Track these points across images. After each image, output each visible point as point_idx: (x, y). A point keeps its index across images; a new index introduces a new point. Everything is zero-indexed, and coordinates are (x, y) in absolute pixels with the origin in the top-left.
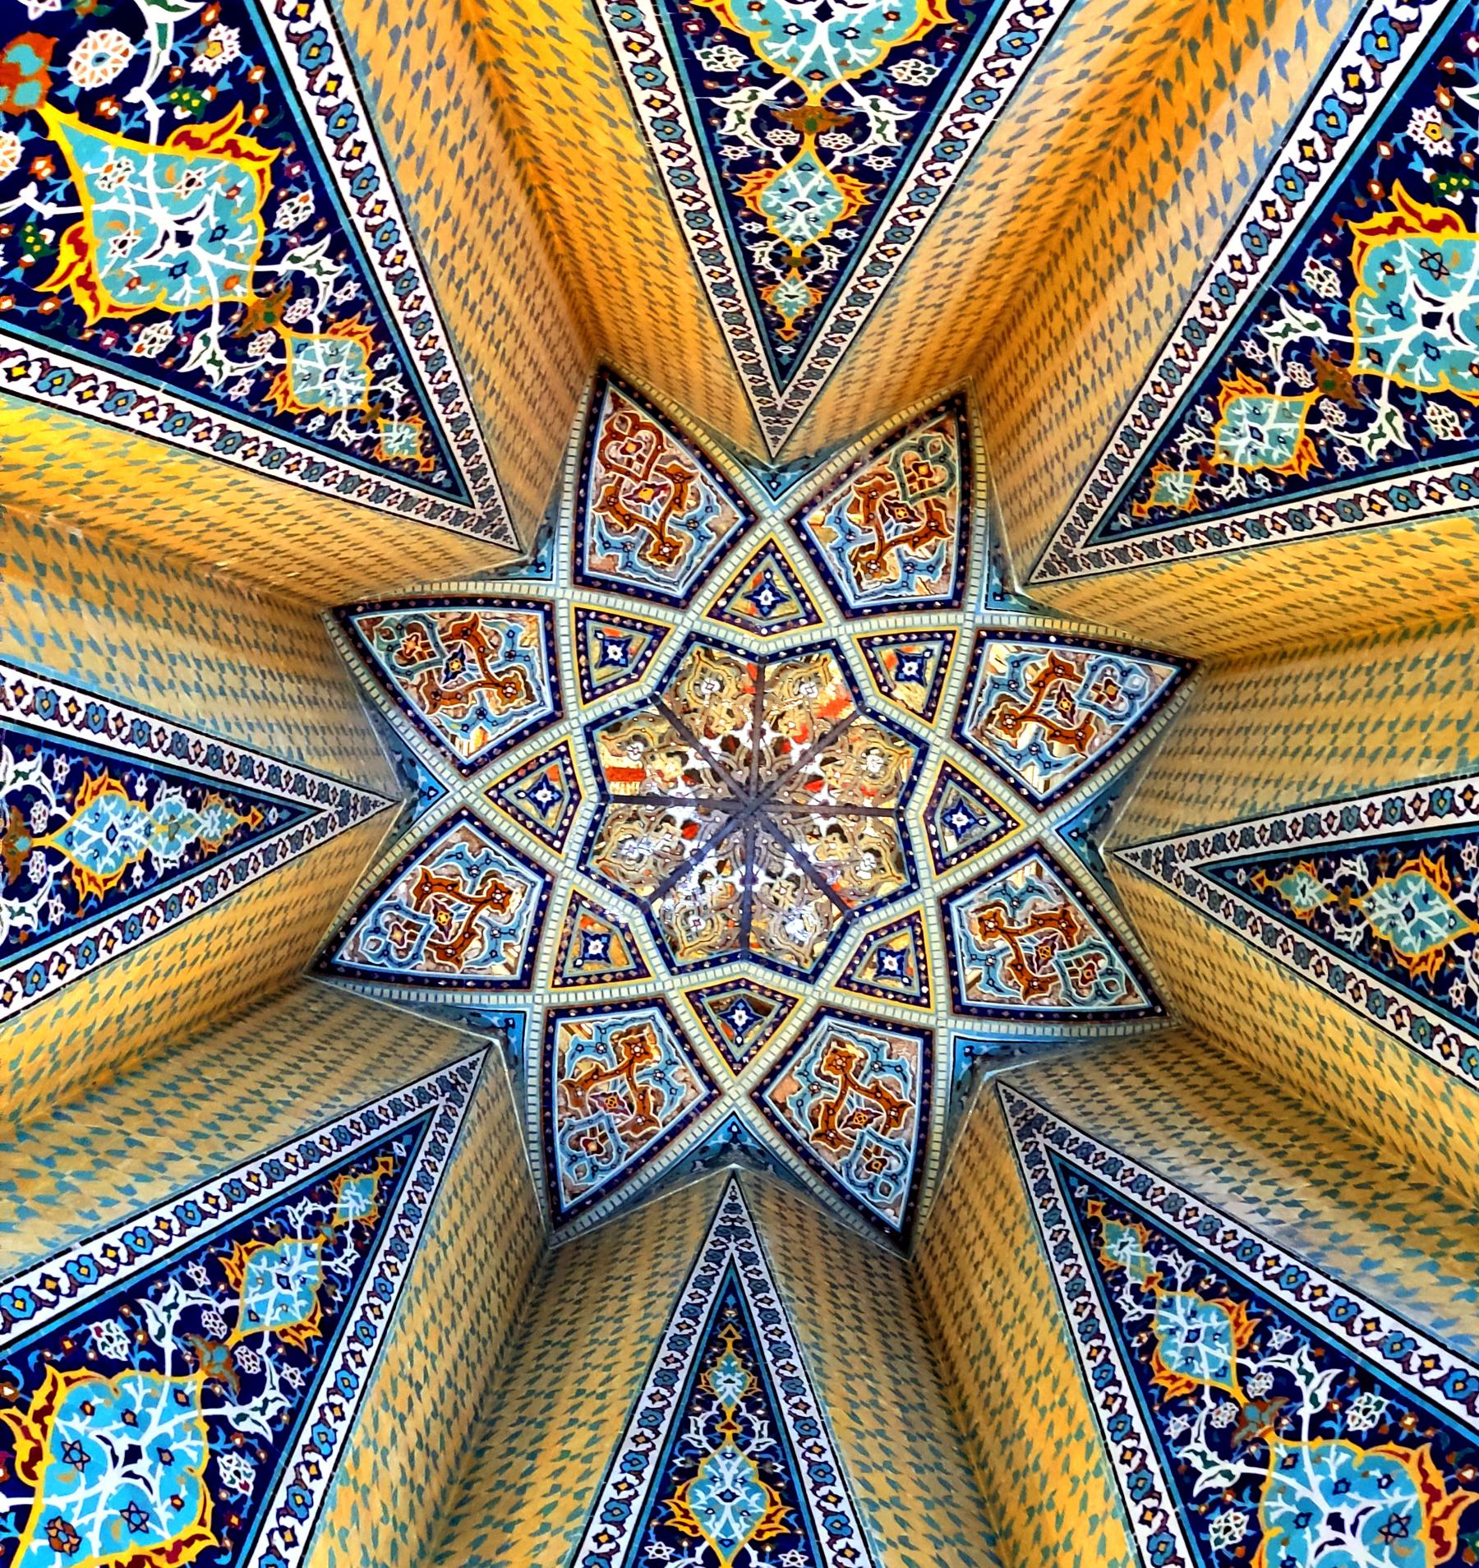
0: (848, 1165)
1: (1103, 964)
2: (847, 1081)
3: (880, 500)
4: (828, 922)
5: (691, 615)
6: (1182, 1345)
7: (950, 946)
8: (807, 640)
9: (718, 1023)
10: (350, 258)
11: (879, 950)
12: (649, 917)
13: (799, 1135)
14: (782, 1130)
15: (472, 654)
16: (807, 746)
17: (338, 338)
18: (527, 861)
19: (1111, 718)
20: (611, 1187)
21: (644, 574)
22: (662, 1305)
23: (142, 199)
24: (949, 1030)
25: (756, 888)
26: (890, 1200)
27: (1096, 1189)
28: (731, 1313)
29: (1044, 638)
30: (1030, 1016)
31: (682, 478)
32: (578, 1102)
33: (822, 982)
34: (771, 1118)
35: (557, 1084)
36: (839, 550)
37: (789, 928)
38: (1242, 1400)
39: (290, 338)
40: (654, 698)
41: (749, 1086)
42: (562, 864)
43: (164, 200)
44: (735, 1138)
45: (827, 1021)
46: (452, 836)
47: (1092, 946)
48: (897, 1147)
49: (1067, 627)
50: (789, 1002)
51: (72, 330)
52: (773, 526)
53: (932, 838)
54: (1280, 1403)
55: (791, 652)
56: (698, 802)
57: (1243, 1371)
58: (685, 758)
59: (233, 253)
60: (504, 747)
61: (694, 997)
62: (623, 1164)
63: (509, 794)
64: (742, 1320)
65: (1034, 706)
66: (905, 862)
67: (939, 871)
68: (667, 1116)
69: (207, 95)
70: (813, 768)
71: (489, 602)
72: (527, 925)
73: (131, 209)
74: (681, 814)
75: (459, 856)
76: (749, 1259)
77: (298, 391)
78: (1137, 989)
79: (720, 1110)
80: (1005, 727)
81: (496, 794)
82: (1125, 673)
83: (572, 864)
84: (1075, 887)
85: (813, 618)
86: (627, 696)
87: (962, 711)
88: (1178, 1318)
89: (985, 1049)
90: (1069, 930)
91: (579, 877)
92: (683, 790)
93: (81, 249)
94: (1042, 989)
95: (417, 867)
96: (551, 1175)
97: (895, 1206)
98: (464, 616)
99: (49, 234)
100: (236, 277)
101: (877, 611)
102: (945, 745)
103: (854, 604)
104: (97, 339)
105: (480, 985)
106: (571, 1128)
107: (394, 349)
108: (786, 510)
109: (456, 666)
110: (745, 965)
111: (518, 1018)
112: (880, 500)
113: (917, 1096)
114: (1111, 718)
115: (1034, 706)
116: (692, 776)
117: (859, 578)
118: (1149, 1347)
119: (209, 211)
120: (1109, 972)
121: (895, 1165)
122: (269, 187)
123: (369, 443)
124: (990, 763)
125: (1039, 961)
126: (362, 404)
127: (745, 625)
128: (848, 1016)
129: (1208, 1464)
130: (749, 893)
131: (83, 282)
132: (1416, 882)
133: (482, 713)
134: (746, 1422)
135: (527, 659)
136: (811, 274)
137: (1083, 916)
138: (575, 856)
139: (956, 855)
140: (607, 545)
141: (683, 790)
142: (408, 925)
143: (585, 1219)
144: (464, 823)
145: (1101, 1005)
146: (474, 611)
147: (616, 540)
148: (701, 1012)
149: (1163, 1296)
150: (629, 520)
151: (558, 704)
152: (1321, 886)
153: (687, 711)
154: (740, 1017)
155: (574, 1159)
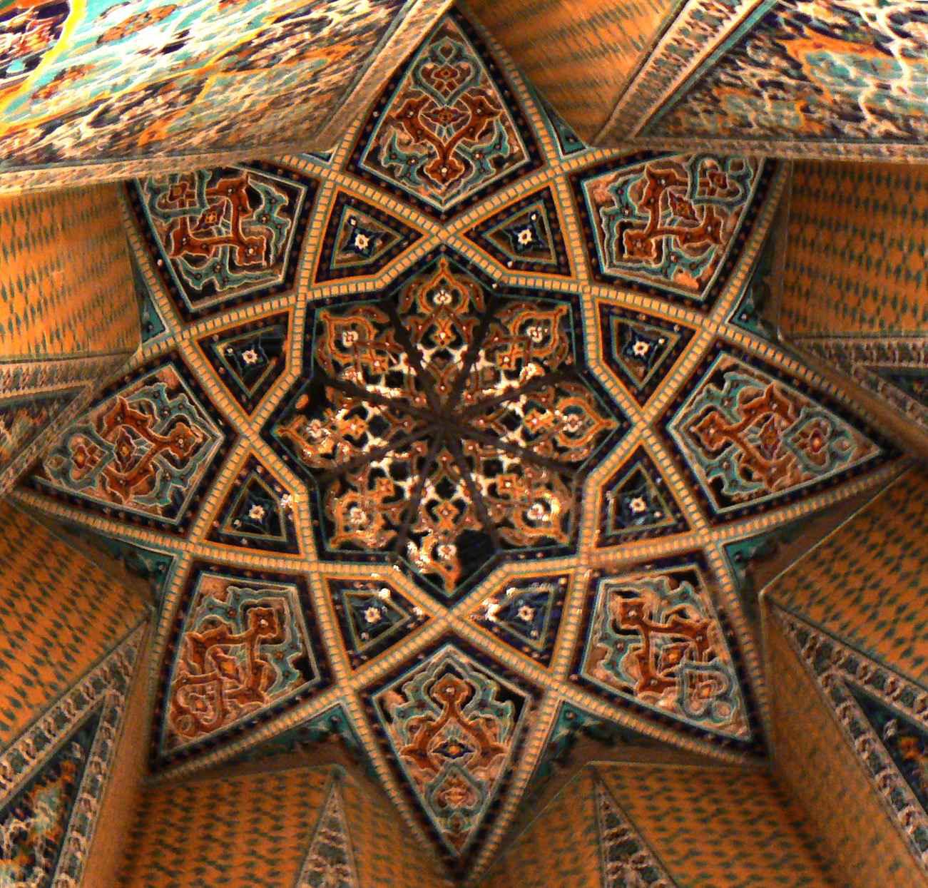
0: (730, 205)
2: (654, 231)
3: (123, 474)
5: (306, 567)
7: (483, 195)
8: (272, 458)
11: (517, 252)
14: (726, 273)
15: (437, 741)
18: (589, 602)
20: (846, 414)
21: (295, 630)
25: (515, 384)
30: (512, 101)
31: (200, 647)
32: (782, 470)
33: (573, 288)
34: (720, 286)
35: (774, 494)
36: (183, 479)
41: (698, 318)
44: (752, 316)
46: (599, 675)
47: (418, 83)
48: (693, 168)
49: (142, 259)
53: (390, 256)
58: (432, 504)
61: (642, 397)
62: (819, 408)
66: (425, 267)
67: (419, 235)
68: (757, 386)
70: (382, 388)
71: (386, 748)
75: (612, 665)
79: (733, 334)
80: (258, 252)
85: (252, 463)
87: (264, 295)
91: (583, 548)
94: (481, 104)
95: (638, 699)
96: (857, 472)
101: (217, 415)
102: (302, 290)
103: (221, 437)
106: (807, 468)
108: (176, 544)
110: (592, 364)
111: (733, 550)
112: (123, 474)
113: (637, 166)
115: (227, 241)
116: (445, 490)
117: (198, 447)
120: (434, 58)
124: (297, 247)
125: (454, 116)
128: (592, 253)
137: (395, 100)
142: (693, 686)
144: (584, 673)
145: (470, 51)
146: (401, 757)
147: (278, 670)
150: (257, 669)
155: (835, 456)
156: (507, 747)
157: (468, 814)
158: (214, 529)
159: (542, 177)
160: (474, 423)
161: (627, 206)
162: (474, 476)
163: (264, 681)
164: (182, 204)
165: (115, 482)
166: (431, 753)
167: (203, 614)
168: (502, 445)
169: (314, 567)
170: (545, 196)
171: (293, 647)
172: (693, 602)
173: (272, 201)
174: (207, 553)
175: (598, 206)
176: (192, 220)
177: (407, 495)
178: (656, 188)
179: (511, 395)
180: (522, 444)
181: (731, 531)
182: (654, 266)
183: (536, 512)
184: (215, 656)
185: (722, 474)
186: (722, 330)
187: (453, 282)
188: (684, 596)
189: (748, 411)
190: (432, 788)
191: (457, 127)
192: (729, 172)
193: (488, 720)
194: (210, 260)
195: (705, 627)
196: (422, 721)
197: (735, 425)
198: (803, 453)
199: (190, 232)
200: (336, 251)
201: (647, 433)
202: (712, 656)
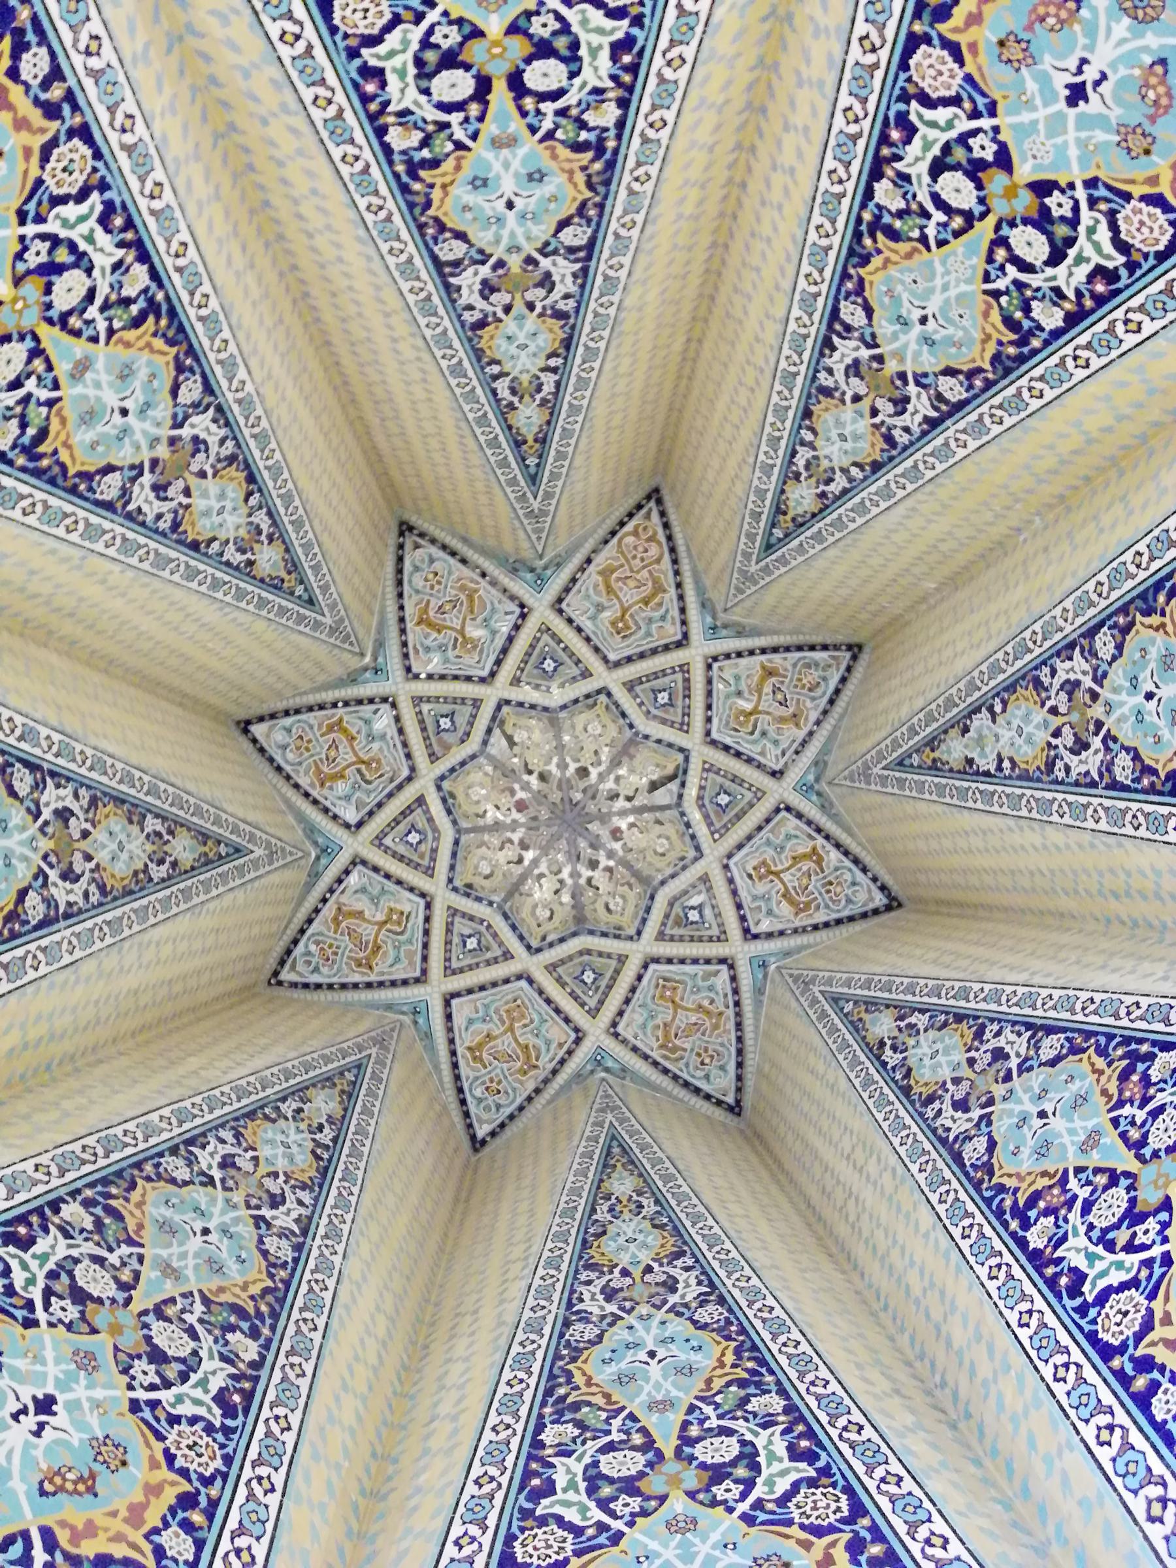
10: (924, 433)
17: (869, 437)
23: (945, 288)
38: (258, 1175)
39: (865, 405)
43: (947, 301)
51: (855, 260)
54: (265, 1196)
57: (276, 1175)
59: (917, 355)
69: (1018, 315)
73: (939, 282)
77: (829, 417)
93: (909, 256)
99: (916, 234)
100: (902, 360)
104: (850, 277)
107: (865, 478)
119: (943, 332)
122: (965, 368)
123: (797, 476)
126: (825, 464)
129: (212, 1155)
131: (887, 261)
149: (303, 1126)
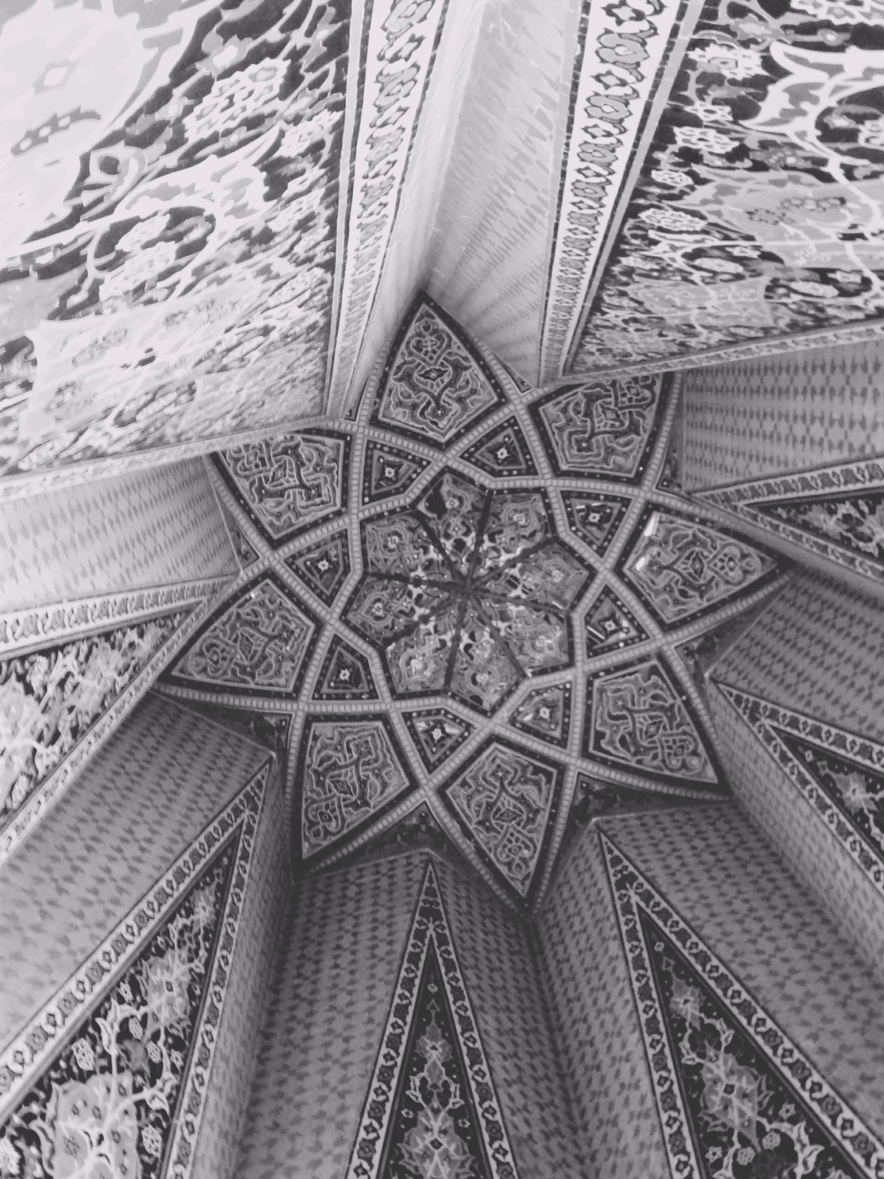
1: (526, 853)
2: (356, 763)
3: (697, 549)
4: (433, 680)
5: (555, 482)
6: (428, 1142)
7: (471, 760)
8: (586, 556)
9: (332, 667)
12: (361, 581)
13: (308, 761)
15: (446, 380)
16: (524, 596)
18: (345, 491)
19: (664, 761)
22: (197, 817)
24: (426, 795)
25: (422, 627)
26: (313, 840)
27: (442, 993)
28: (225, 861)
29: (682, 691)
31: (634, 428)
32: (233, 628)
33: (398, 704)
34: (304, 738)
35: (233, 609)
37: (380, 613)
40: (491, 491)
41: (312, 709)
42: (358, 511)
45: (379, 724)
46: (329, 441)
47: (531, 840)
48: (343, 820)
49: (697, 702)
50: (373, 695)
52: (640, 496)
55: (572, 551)
56: (447, 558)
58: (466, 534)
60: (403, 432)
61: (337, 640)
62: (219, 682)
63: (377, 454)
64: (228, 871)
65: (638, 712)
68: (261, 681)
71: (485, 368)
72: (309, 519)
74: (433, 554)
76: (250, 831)
78: (528, 883)
80: (615, 703)
81: (371, 446)
82: (695, 753)
83: (361, 516)
84: (556, 805)
85: (601, 551)
86: (482, 478)
87: (608, 671)
88: (436, 1124)
89: (432, 824)
90: (530, 821)
92: (449, 545)
94: (489, 829)
97: (313, 846)
98: (466, 359)
101: (631, 586)
102: (580, 675)
103: (625, 569)
105: (256, 522)
109: (433, 375)
110: (374, 654)
112: (697, 549)
114: (664, 761)
115: (638, 712)
116: (460, 545)
118: (412, 1123)
120: (524, 860)
121: (333, 826)
127: (570, 515)
130: (416, 624)
132: (748, 1083)
133: (414, 406)
134: (198, 943)
135: (465, 409)
136: (849, 535)
138: (367, 514)
139: (523, 724)
140: (565, 410)
141: (449, 545)
142: (262, 460)
143: (173, 690)
144: (342, 443)
145: (504, 870)
146: (473, 363)
147: (572, 413)
148: (331, 651)
150: (588, 414)
151: (450, 443)
152: (697, 1013)
153: (497, 516)
154: (345, 675)
155: (201, 654)
156: (391, 382)
157: (419, 335)
158: (627, 506)
159: (435, 781)
160: (446, 595)
161: (377, 776)
162: (440, 557)
163: (583, 405)
164: (674, 742)
165: (704, 545)
166: (450, 369)
167: (631, 451)
168: (425, 583)
169: (548, 483)
170: (431, 767)
171: (561, 430)
172: (271, 514)
173: (611, 743)
174: (630, 490)
175: (396, 768)
176: (665, 728)
177: (486, 537)
178: (363, 794)
179: (425, 619)
180: (410, 587)
181: (256, 571)
182: (349, 737)
183: (394, 542)
184: (622, 424)
185: (271, 607)
186: (295, 707)
187: (476, 690)
188: (279, 516)
189: (264, 657)
190: (449, 346)
191: (499, 810)
192: (320, 827)
193: (409, 397)
194: (647, 698)
195: (261, 501)
196: (461, 388)
197: (272, 645)
198: (222, 646)
199: (665, 720)
200: (561, 704)
201: (328, 617)
202: (252, 484)
